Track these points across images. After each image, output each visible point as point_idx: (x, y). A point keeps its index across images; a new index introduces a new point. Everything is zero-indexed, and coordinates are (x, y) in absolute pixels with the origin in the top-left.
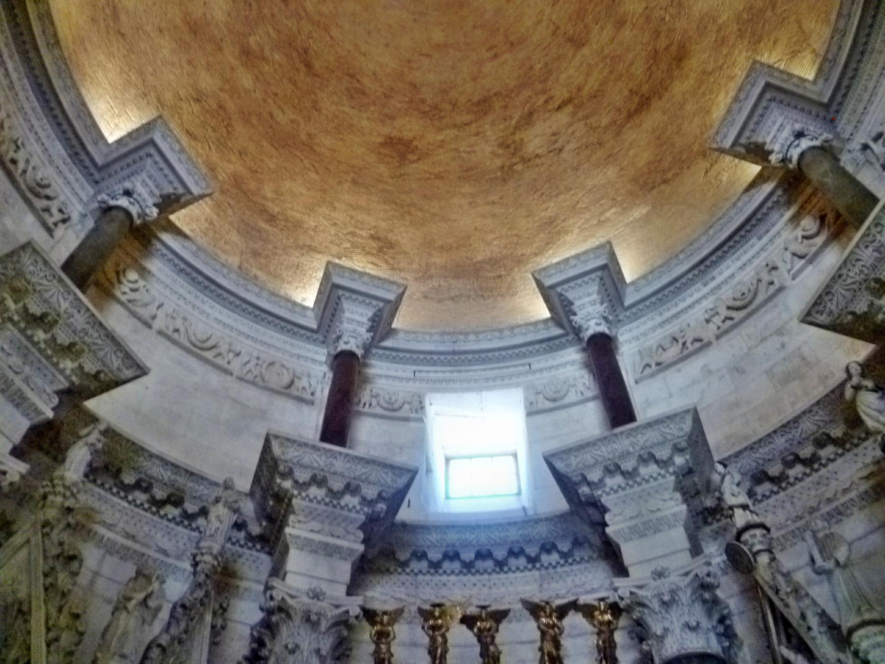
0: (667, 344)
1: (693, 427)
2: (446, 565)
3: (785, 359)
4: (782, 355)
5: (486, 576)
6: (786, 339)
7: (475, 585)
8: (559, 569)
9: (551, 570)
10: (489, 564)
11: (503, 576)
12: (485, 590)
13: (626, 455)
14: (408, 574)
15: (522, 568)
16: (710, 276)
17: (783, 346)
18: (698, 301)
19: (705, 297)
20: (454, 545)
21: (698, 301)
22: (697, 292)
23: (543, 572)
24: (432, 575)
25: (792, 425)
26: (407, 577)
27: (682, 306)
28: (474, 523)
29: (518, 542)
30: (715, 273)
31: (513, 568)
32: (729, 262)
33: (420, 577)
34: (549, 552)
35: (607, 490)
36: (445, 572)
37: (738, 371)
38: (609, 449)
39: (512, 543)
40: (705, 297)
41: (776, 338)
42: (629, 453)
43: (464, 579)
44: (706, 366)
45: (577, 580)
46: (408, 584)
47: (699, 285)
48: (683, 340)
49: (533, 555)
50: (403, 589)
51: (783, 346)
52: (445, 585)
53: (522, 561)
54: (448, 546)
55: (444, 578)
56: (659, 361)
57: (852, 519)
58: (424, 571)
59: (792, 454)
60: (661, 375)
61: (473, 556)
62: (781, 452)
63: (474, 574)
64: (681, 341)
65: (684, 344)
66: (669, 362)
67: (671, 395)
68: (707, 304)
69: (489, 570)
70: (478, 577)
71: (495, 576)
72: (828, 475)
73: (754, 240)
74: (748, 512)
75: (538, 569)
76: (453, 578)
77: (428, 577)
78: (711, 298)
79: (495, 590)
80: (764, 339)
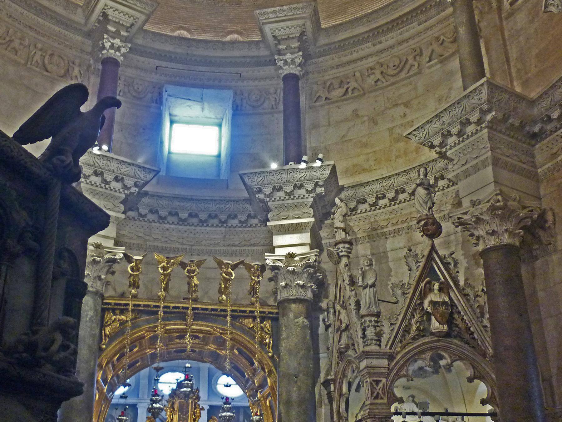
0: (336, 85)
1: (331, 173)
2: (170, 219)
3: (402, 125)
4: (402, 121)
5: (193, 228)
6: (408, 111)
7: (186, 231)
8: (237, 229)
9: (232, 229)
10: (195, 221)
11: (203, 228)
12: (192, 235)
13: (287, 182)
14: (146, 222)
15: (215, 225)
16: (379, 40)
17: (405, 115)
18: (366, 57)
19: (371, 55)
20: (176, 209)
21: (366, 57)
22: (367, 48)
23: (227, 229)
24: (161, 223)
25: (387, 179)
26: (145, 223)
27: (355, 56)
28: (190, 197)
29: (215, 211)
30: (383, 39)
31: (210, 225)
32: (393, 34)
33: (153, 224)
34: (233, 218)
35: (273, 199)
36: (168, 222)
37: (374, 122)
38: (279, 177)
39: (212, 211)
40: (371, 55)
41: (402, 106)
42: (289, 182)
43: (180, 227)
44: (356, 110)
45: (246, 236)
46: (145, 227)
47: (370, 44)
48: (348, 86)
49: (223, 220)
50: (142, 230)
51: (405, 115)
52: (168, 230)
53: (215, 222)
54: (172, 208)
55: (167, 226)
56: (328, 96)
57: (401, 237)
58: (156, 221)
59: (383, 194)
60: (327, 107)
61: (187, 215)
62: (377, 192)
63: (186, 225)
64: (346, 86)
65: (347, 89)
66: (335, 99)
67: (329, 125)
68: (370, 63)
69: (195, 224)
70: (188, 227)
71: (198, 228)
72: (398, 210)
73: (415, 24)
74: (344, 233)
75: (225, 227)
76: (173, 226)
77: (157, 225)
78: (374, 58)
79: (197, 236)
80: (396, 105)
